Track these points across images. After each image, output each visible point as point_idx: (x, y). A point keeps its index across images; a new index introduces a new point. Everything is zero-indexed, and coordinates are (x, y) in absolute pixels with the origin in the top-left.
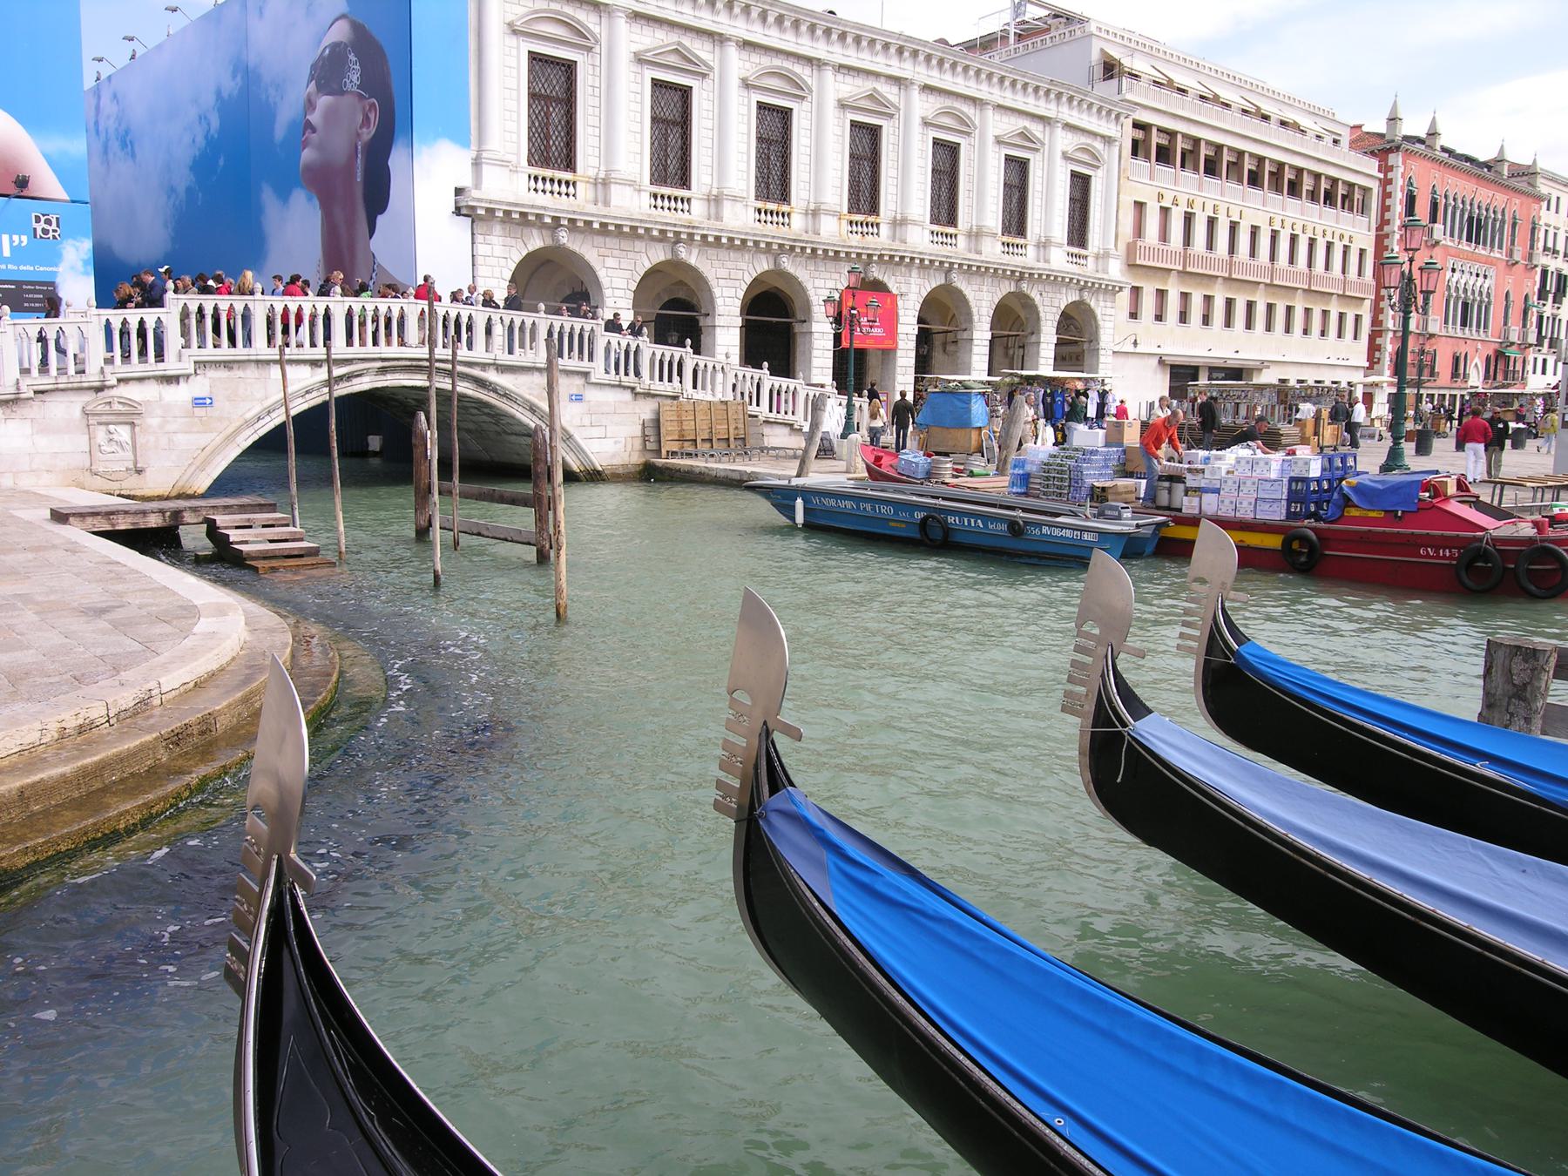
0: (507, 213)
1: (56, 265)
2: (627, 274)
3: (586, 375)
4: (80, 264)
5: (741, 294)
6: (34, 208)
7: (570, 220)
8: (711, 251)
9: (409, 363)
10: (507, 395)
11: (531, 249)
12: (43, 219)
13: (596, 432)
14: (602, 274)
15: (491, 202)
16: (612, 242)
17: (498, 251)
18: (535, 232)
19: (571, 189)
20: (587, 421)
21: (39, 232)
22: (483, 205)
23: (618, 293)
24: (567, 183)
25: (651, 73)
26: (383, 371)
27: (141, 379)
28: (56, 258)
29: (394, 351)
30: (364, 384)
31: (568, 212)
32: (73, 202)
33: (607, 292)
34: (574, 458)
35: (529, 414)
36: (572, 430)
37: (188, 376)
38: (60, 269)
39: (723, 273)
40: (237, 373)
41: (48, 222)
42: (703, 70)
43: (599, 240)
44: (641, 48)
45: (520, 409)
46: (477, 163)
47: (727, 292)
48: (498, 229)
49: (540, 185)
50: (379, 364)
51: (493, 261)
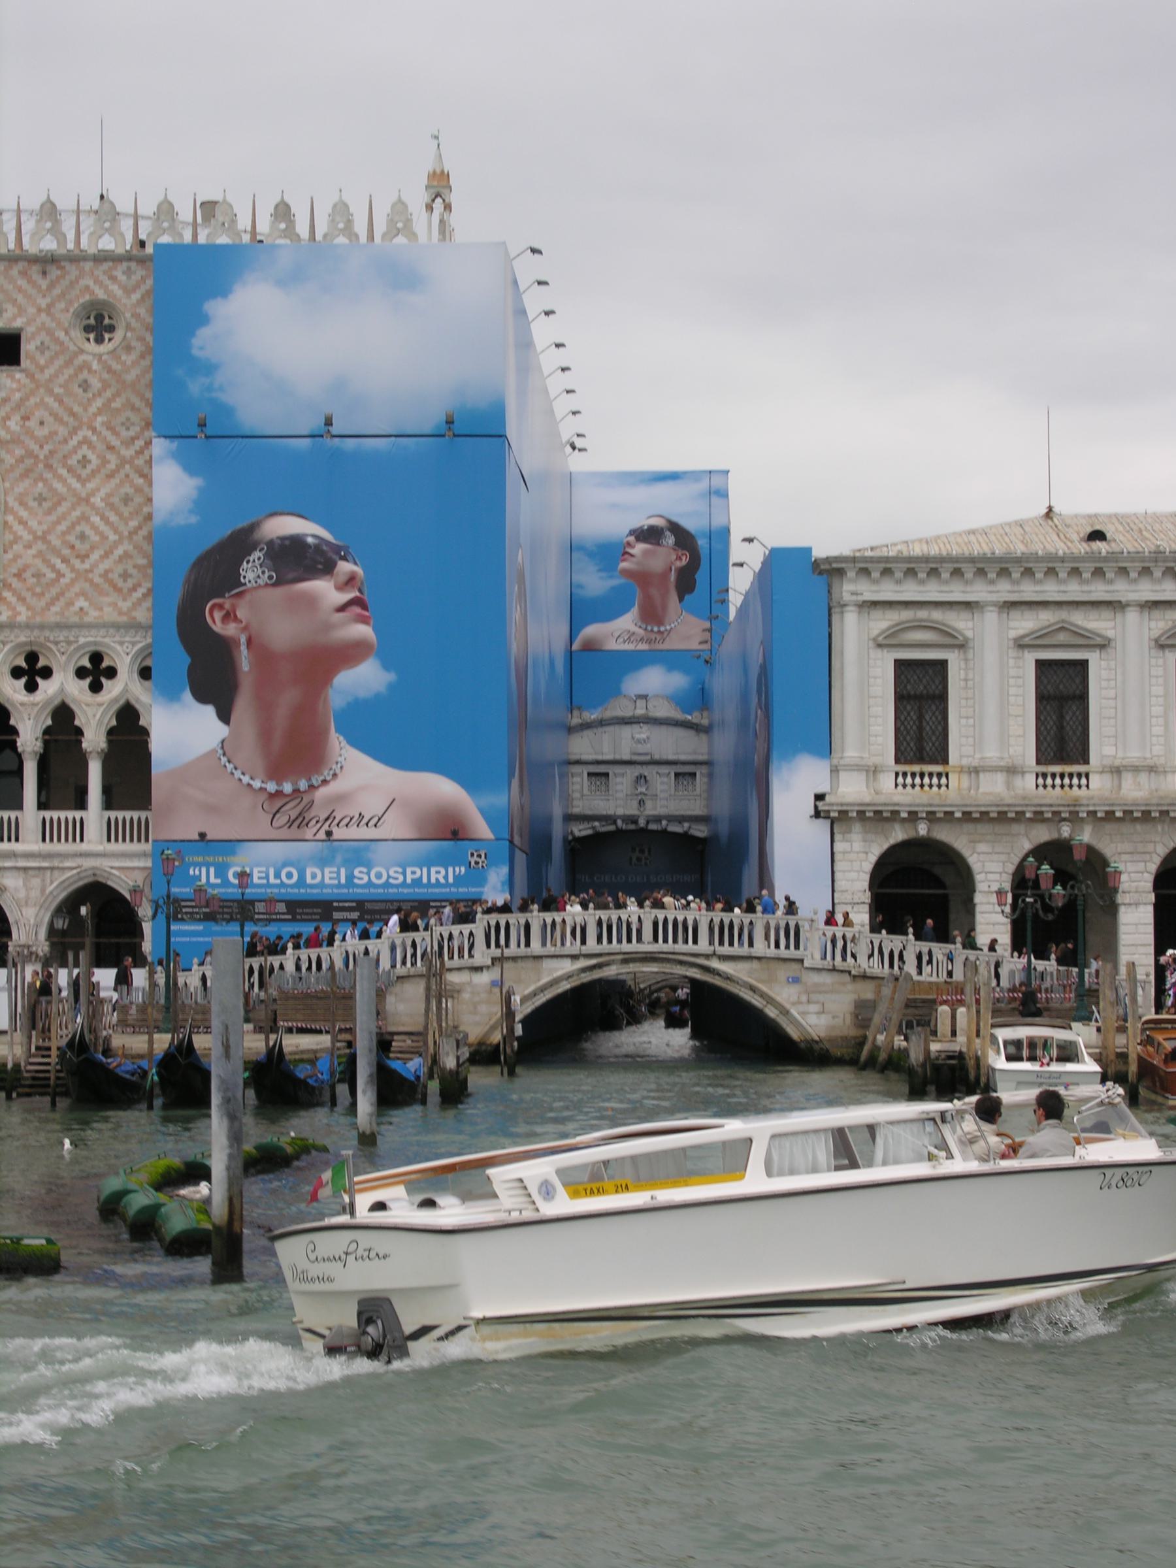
0: (861, 813)
1: (483, 886)
2: (1003, 857)
3: (802, 961)
4: (499, 885)
5: (1153, 867)
6: (469, 847)
7: (928, 813)
8: (1109, 827)
9: (644, 955)
10: (728, 978)
11: (892, 841)
12: (475, 854)
13: (813, 1008)
14: (973, 860)
15: (842, 805)
16: (982, 828)
17: (858, 845)
18: (897, 826)
19: (943, 781)
20: (804, 998)
21: (473, 863)
22: (835, 808)
23: (990, 876)
24: (939, 775)
25: (1029, 659)
26: (625, 961)
27: (459, 969)
28: (481, 881)
29: (634, 947)
30: (611, 972)
31: (924, 805)
32: (497, 839)
33: (978, 878)
34: (794, 1029)
35: (751, 993)
36: (788, 1006)
37: (488, 967)
38: (486, 889)
39: (1127, 847)
40: (520, 964)
41: (480, 856)
42: (1099, 640)
43: (969, 827)
44: (1021, 632)
45: (743, 989)
46: (835, 770)
47: (1131, 867)
48: (857, 827)
49: (909, 780)
50: (620, 957)
51: (853, 856)
